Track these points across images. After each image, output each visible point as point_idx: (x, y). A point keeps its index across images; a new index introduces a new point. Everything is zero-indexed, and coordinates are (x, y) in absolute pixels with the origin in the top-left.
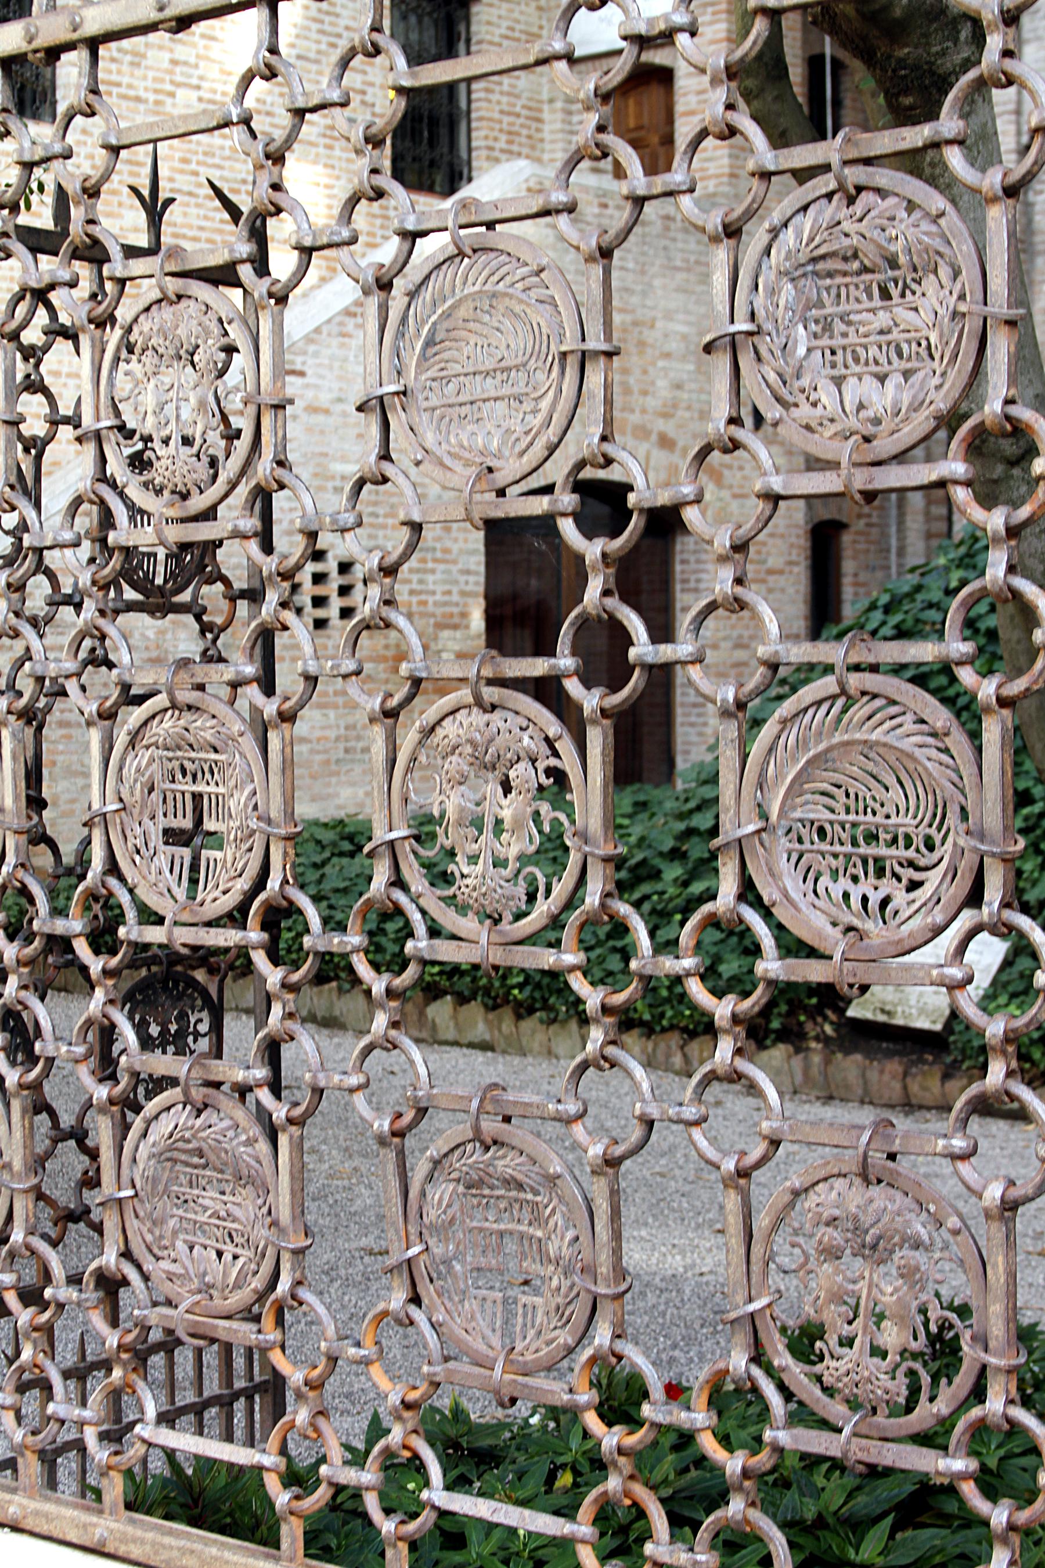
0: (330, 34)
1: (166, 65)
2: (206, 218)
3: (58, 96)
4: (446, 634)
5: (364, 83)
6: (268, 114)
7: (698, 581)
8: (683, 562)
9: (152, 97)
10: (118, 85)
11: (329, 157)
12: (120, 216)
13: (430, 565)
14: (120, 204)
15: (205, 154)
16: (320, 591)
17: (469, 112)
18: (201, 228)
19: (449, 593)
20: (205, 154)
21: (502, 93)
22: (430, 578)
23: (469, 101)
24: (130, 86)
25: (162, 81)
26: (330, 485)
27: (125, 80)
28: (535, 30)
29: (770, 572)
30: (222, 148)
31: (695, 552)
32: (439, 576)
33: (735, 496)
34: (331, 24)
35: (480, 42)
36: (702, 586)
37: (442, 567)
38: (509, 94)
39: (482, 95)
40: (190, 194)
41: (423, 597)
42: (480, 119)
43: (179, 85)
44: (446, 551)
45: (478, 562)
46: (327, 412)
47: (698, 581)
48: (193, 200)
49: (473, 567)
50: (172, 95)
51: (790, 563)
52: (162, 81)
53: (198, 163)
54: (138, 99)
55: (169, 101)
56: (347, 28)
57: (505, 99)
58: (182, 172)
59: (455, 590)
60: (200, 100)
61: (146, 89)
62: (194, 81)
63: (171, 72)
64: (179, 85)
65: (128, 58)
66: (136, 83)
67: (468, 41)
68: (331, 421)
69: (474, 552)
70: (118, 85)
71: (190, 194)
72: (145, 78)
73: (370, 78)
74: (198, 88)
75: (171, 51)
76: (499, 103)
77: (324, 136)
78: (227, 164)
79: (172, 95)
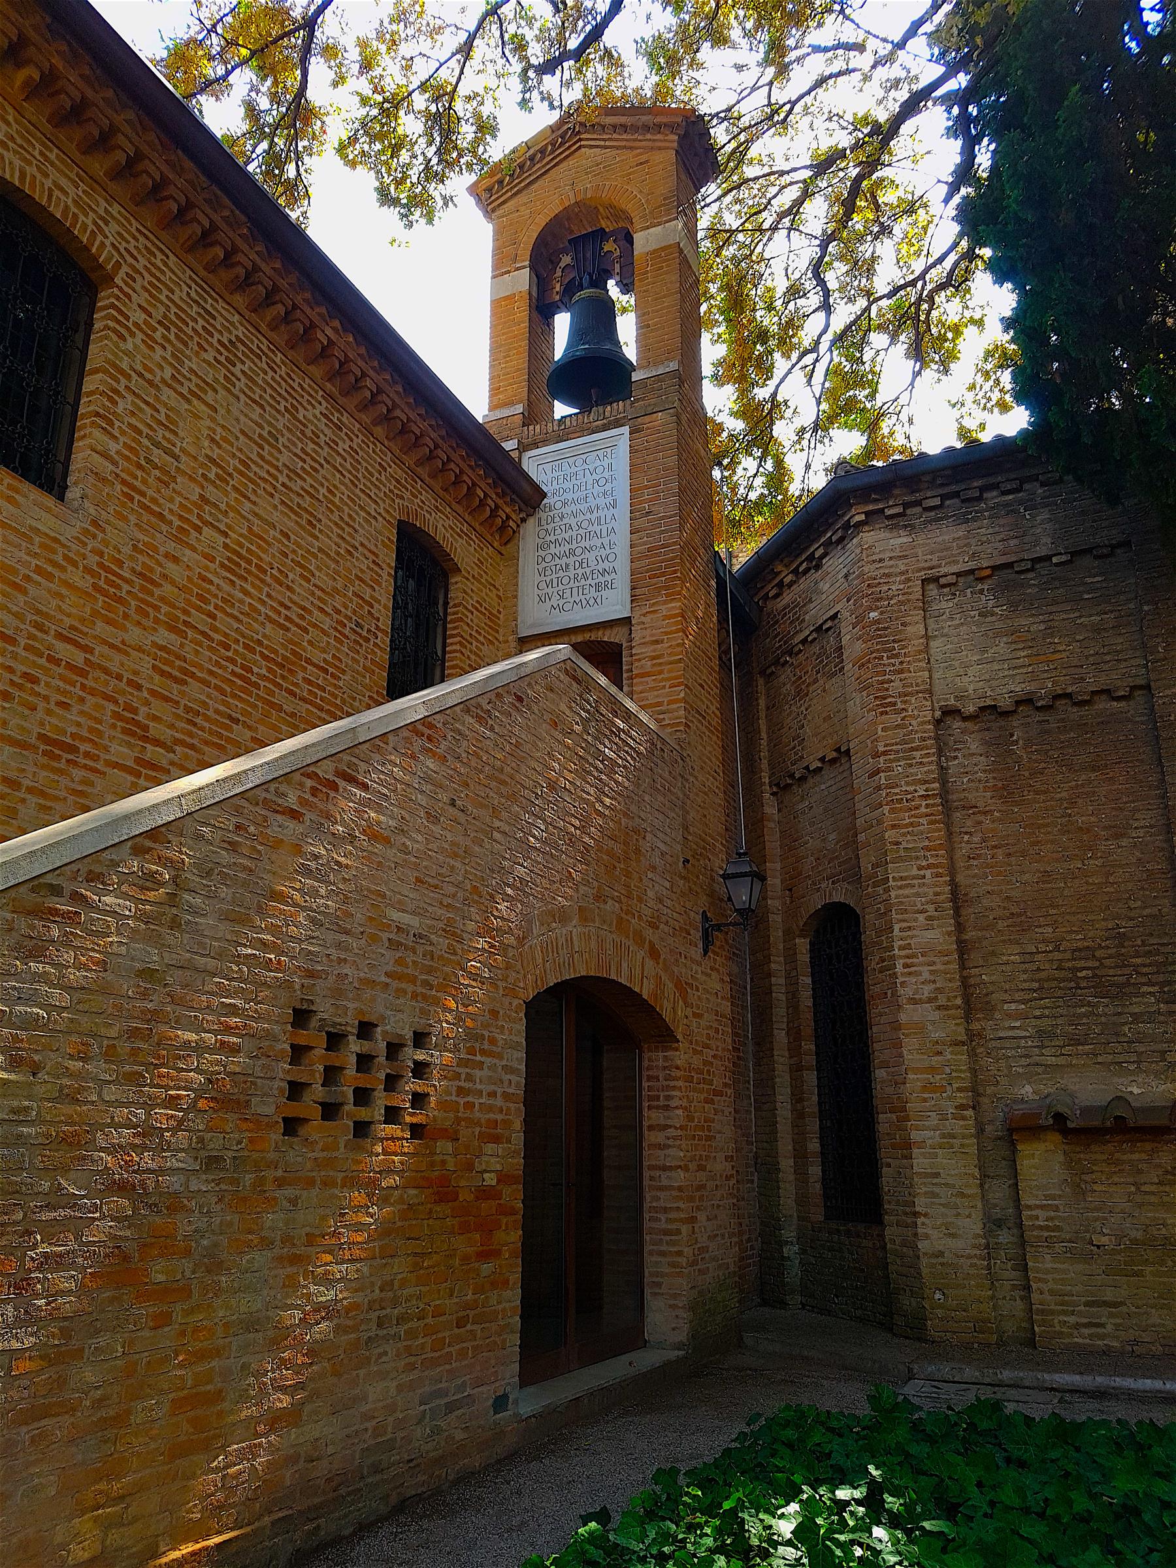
0: (348, 543)
1: (195, 497)
2: (217, 664)
3: (70, 480)
4: (490, 1148)
5: (372, 597)
6: (289, 588)
7: (668, 1098)
8: (649, 1078)
9: (177, 523)
10: (143, 494)
11: (338, 650)
12: (125, 630)
13: (478, 1058)
14: (126, 616)
15: (224, 600)
16: (363, 1081)
17: (443, 661)
18: (211, 673)
19: (492, 1094)
20: (224, 600)
21: (471, 651)
22: (478, 1073)
23: (444, 652)
24: (154, 500)
25: (190, 511)
26: (385, 936)
27: (150, 492)
28: (495, 612)
29: (717, 1093)
30: (241, 602)
31: (665, 1068)
32: (486, 1072)
33: (695, 1015)
34: (349, 534)
35: (455, 606)
36: (673, 1103)
37: (488, 1060)
38: (475, 654)
39: (458, 647)
40: (203, 633)
41: (470, 1099)
42: (453, 667)
43: (206, 523)
44: (493, 1041)
45: (518, 1058)
46: (387, 841)
47: (668, 1098)
48: (206, 642)
49: (515, 1065)
50: (198, 530)
51: (725, 1085)
52: (190, 511)
53: (216, 607)
54: (161, 516)
55: (194, 534)
56: (362, 544)
57: (473, 657)
58: (199, 609)
59: (499, 1091)
60: (226, 546)
61: (171, 510)
62: (222, 527)
63: (200, 508)
64: (206, 523)
65: (157, 473)
66: (162, 501)
67: (446, 603)
68: (390, 853)
69: (515, 1046)
70: (143, 494)
71: (203, 633)
72: (171, 500)
73: (376, 595)
74: (226, 535)
75: (203, 488)
76: (469, 657)
77: (336, 629)
78: (245, 620)
79: (198, 530)
